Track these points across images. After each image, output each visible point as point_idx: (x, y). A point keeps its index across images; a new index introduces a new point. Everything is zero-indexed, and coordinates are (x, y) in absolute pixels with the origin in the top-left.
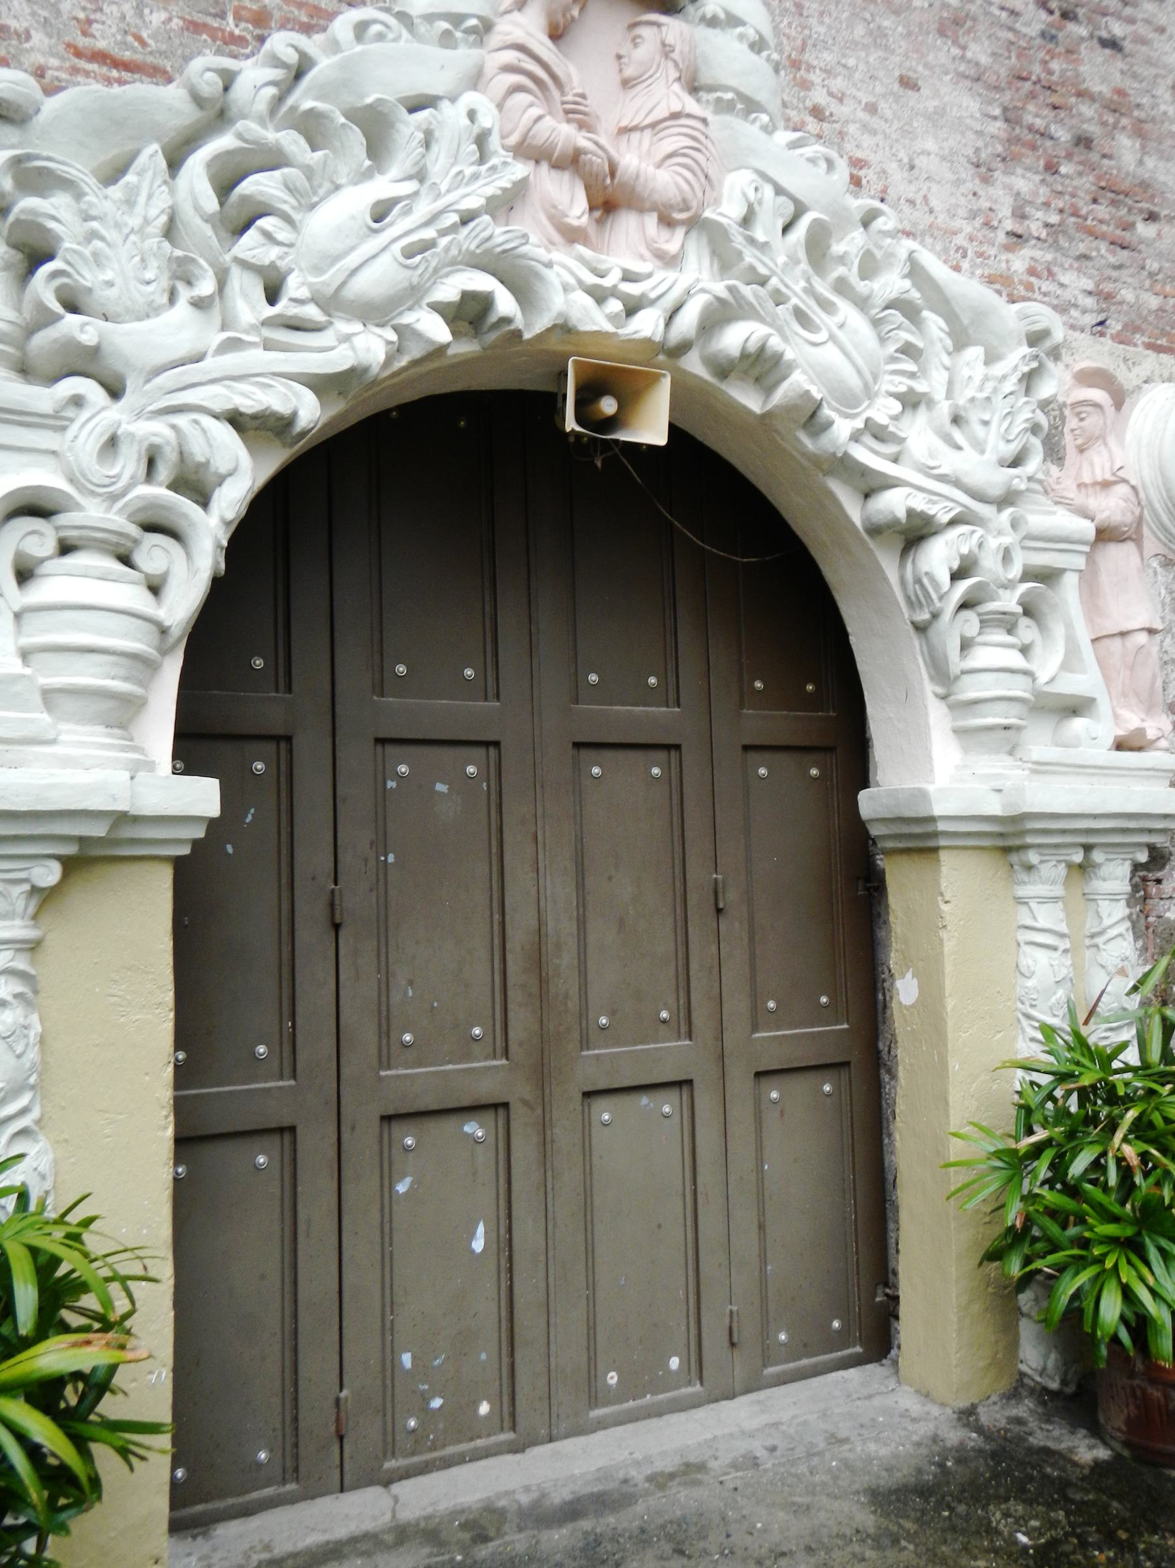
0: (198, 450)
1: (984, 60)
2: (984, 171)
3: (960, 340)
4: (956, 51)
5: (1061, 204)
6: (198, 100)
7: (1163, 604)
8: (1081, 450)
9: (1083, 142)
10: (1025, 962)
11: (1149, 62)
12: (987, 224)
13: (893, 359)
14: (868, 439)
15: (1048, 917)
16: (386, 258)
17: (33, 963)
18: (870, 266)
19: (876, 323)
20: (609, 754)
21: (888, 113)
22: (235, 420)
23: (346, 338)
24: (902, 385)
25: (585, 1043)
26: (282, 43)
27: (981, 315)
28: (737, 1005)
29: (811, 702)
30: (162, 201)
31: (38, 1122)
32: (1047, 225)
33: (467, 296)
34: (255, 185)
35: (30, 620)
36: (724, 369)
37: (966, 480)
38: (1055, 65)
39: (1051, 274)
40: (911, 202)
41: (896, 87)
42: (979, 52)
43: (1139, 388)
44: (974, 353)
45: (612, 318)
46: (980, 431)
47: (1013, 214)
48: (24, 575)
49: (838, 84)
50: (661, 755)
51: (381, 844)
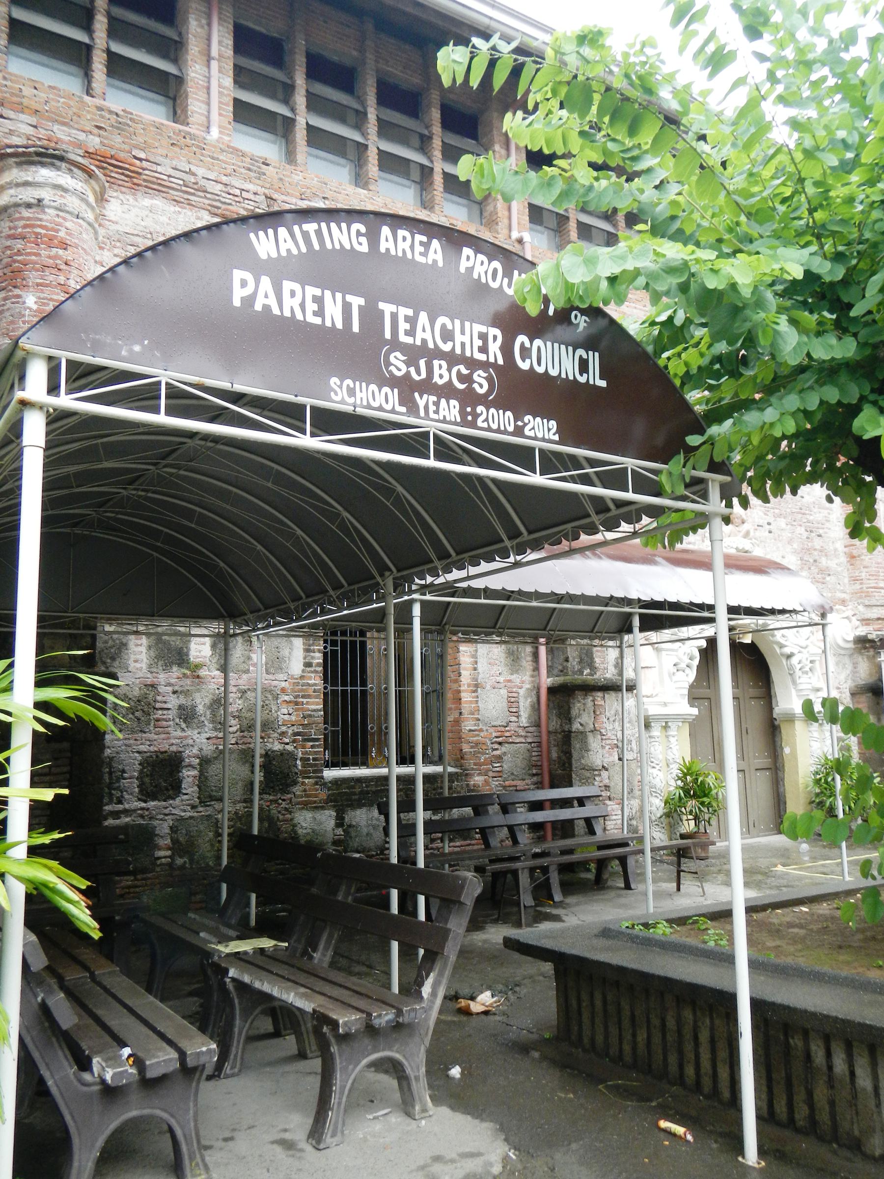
9: (815, 561)
15: (816, 734)
28: (751, 754)
29: (760, 687)
42: (795, 546)
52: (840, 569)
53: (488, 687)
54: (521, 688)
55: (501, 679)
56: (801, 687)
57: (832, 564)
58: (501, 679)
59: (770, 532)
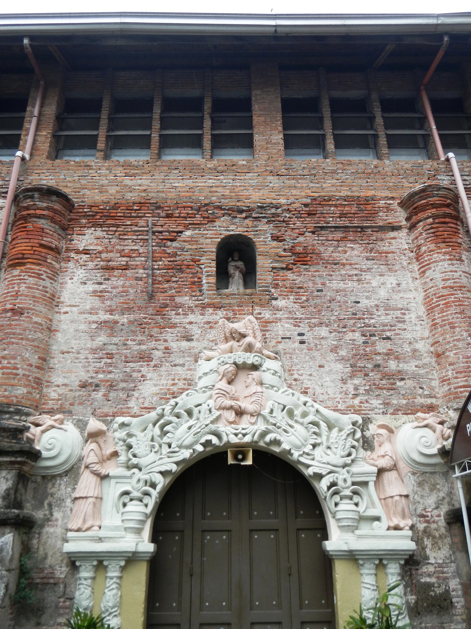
0: (153, 480)
1: (344, 354)
2: (344, 381)
3: (330, 427)
4: (336, 355)
5: (369, 384)
6: (158, 415)
7: (413, 486)
8: (380, 446)
10: (363, 593)
11: (400, 339)
12: (346, 394)
13: (311, 436)
14: (305, 456)
16: (190, 437)
17: (120, 581)
18: (305, 415)
19: (306, 428)
20: (259, 532)
21: (315, 375)
22: (161, 473)
23: (182, 453)
24: (313, 442)
25: (251, 609)
26: (172, 402)
27: (337, 420)
30: (151, 434)
31: (119, 614)
32: (365, 390)
33: (207, 441)
34: (166, 428)
35: (124, 515)
36: (268, 444)
37: (331, 463)
38: (368, 349)
39: (367, 402)
40: (323, 394)
41: (318, 368)
42: (343, 353)
43: (401, 426)
44: (336, 430)
46: (334, 450)
47: (354, 389)
48: (125, 505)
49: (300, 372)
50: (274, 532)
51: (202, 556)
52: (422, 371)
56: (339, 516)
59: (302, 342)
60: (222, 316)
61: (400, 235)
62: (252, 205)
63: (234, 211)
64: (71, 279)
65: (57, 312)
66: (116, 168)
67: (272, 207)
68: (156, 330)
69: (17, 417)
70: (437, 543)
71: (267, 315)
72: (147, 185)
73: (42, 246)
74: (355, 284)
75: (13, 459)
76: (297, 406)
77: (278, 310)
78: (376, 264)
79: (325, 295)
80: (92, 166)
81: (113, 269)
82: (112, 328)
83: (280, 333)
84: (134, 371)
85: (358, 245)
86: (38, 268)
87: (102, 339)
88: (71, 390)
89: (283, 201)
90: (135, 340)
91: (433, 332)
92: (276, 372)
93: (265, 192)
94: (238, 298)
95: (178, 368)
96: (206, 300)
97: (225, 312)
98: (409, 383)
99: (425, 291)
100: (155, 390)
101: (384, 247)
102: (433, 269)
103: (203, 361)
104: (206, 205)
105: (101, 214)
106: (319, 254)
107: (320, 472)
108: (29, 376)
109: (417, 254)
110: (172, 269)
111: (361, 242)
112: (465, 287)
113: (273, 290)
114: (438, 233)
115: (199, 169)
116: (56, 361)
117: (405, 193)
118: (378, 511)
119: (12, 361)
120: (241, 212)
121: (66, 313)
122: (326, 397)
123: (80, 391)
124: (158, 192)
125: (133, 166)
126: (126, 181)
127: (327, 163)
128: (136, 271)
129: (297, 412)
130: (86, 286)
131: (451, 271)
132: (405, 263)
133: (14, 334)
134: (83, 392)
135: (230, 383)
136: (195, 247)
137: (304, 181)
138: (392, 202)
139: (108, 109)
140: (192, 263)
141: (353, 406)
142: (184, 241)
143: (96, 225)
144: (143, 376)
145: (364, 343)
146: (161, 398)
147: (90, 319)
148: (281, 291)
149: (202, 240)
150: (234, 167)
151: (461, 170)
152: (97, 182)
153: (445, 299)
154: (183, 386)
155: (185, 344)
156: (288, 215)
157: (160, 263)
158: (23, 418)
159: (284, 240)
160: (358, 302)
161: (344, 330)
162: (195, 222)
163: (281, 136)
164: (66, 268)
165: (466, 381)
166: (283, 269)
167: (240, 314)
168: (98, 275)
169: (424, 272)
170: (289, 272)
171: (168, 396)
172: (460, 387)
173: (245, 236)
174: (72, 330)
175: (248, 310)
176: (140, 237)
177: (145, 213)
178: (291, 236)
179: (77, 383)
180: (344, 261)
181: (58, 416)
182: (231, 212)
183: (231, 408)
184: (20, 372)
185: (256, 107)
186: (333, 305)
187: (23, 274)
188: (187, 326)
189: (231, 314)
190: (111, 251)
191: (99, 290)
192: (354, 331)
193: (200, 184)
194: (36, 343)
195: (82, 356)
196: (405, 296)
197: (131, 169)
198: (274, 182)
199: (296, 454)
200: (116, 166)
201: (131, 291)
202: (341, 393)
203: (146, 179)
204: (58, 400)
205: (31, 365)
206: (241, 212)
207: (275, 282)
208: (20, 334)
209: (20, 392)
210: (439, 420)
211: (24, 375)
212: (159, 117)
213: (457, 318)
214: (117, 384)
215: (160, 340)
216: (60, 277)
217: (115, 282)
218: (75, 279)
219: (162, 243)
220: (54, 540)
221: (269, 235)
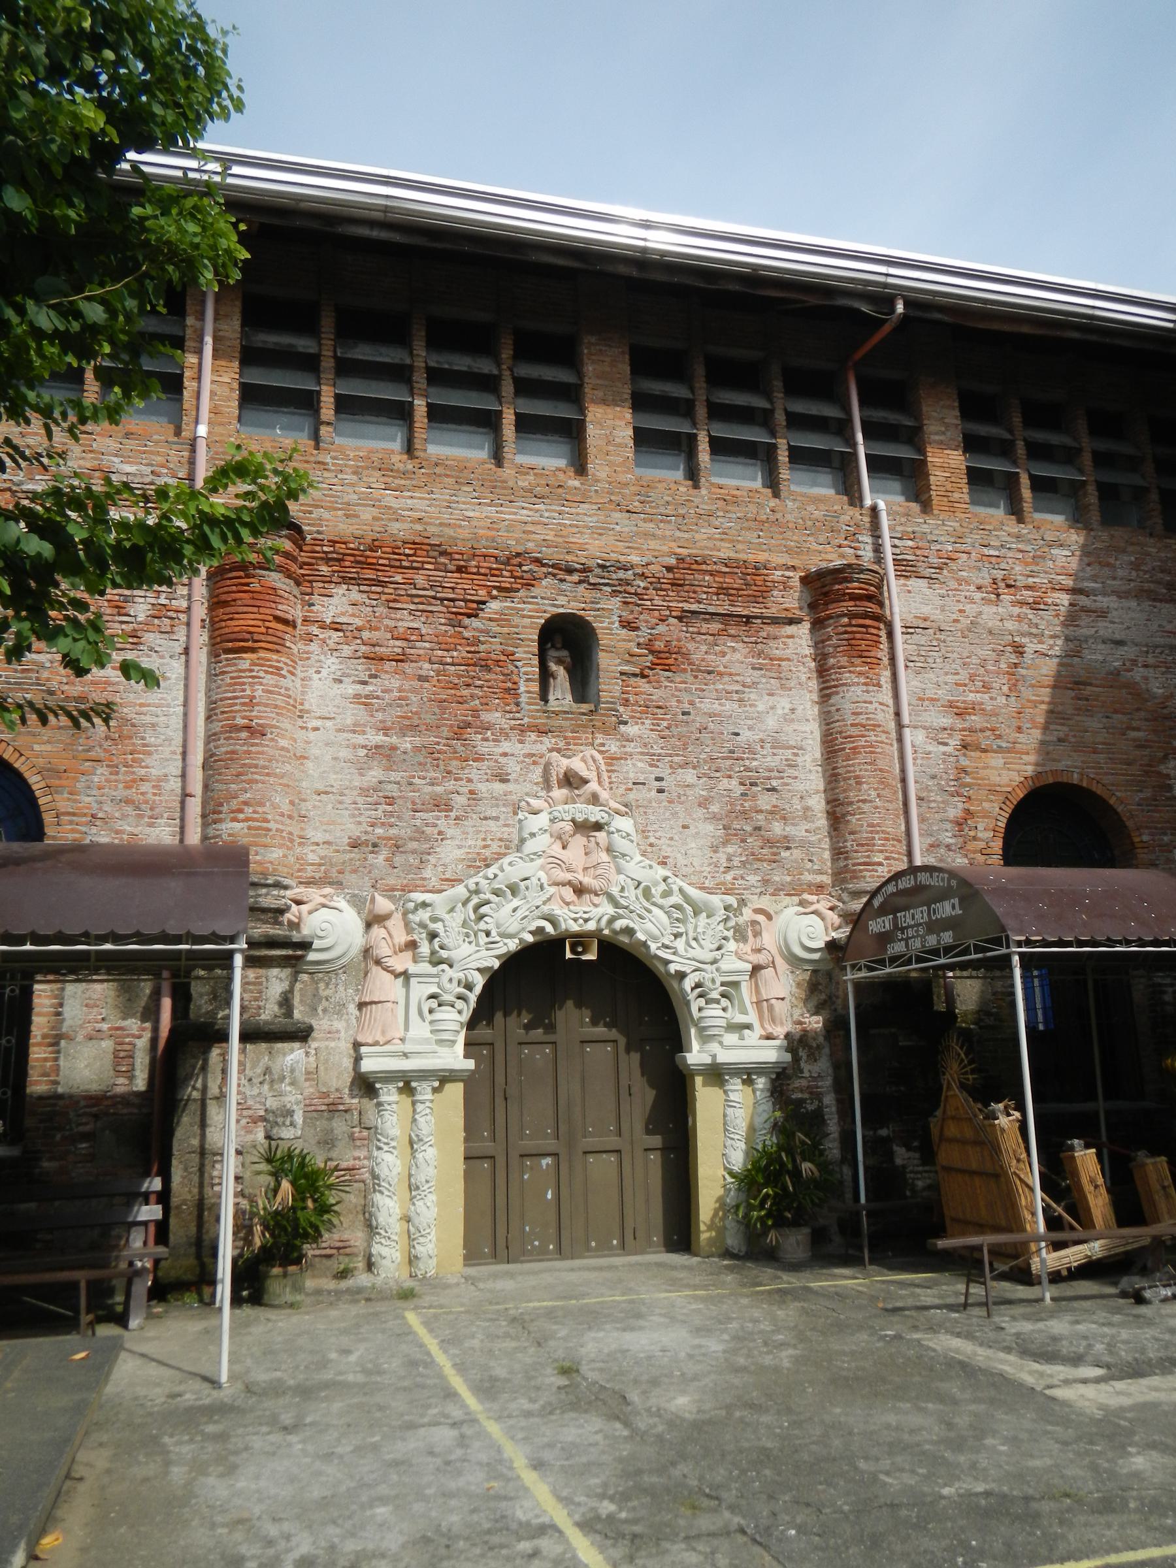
0: (470, 980)
22: (478, 969)
24: (675, 931)
26: (490, 872)
27: (706, 904)
34: (483, 910)
38: (746, 804)
42: (715, 808)
44: (704, 914)
45: (580, 926)
49: (657, 835)
53: (80, 1038)
54: (139, 1037)
55: (105, 1026)
57: (798, 831)
58: (105, 1026)
59: (661, 791)
60: (549, 746)
61: (801, 632)
62: (591, 563)
63: (561, 569)
64: (318, 672)
65: (302, 728)
66: (370, 472)
67: (619, 569)
68: (454, 763)
69: (275, 893)
70: (813, 1054)
71: (613, 747)
72: (422, 511)
73: (278, 619)
74: (735, 706)
75: (290, 952)
76: (656, 884)
77: (628, 740)
78: (764, 676)
79: (693, 721)
80: (326, 464)
81: (382, 659)
82: (389, 757)
83: (631, 775)
84: (427, 825)
85: (741, 645)
86: (275, 657)
87: (375, 774)
88: (338, 851)
89: (635, 559)
90: (424, 778)
91: (833, 785)
92: (628, 835)
93: (608, 540)
94: (571, 719)
95: (490, 822)
96: (526, 720)
97: (553, 740)
98: (797, 853)
99: (828, 724)
100: (460, 853)
101: (775, 649)
102: (842, 695)
103: (527, 814)
104: (518, 555)
105: (352, 559)
106: (686, 655)
107: (683, 969)
108: (282, 831)
109: (821, 666)
110: (474, 665)
111: (746, 639)
112: (879, 726)
113: (621, 709)
114: (853, 642)
115: (505, 488)
116: (309, 805)
117: (815, 564)
118: (752, 1017)
119: (260, 809)
120: (570, 571)
121: (316, 729)
122: (690, 870)
123: (351, 852)
124: (441, 524)
125: (398, 471)
126: (388, 499)
127: (702, 497)
128: (419, 664)
129: (656, 891)
130: (341, 685)
131: (865, 702)
132: (803, 678)
133: (256, 766)
134: (355, 854)
135: (564, 848)
136: (506, 630)
137: (667, 526)
138: (791, 574)
139: (332, 337)
140: (503, 658)
141: (724, 884)
142: (490, 620)
143: (345, 580)
144: (440, 833)
145: (742, 794)
146: (469, 866)
147: (353, 741)
148: (633, 711)
149: (516, 620)
150: (560, 490)
151: (891, 529)
152: (338, 497)
153: (853, 742)
154: (498, 850)
155: (498, 787)
156: (642, 584)
157: (455, 654)
158: (282, 892)
159: (637, 629)
160: (737, 734)
161: (718, 775)
162: (503, 585)
163: (630, 432)
164: (307, 653)
165: (868, 857)
166: (635, 675)
167: (575, 744)
168: (360, 668)
169: (829, 696)
170: (644, 680)
171: (478, 864)
172: (860, 864)
173: (581, 617)
174: (328, 757)
175: (587, 738)
176: (421, 607)
177: (423, 563)
178: (647, 622)
179: (346, 841)
180: (721, 669)
181: (328, 890)
182: (556, 571)
183: (569, 883)
184: (272, 825)
185: (589, 369)
186: (705, 736)
187: (256, 668)
188: (501, 759)
189: (561, 745)
190: (377, 629)
191: (363, 693)
192: (730, 777)
193: (507, 517)
194: (285, 781)
195: (348, 799)
196: (800, 728)
197: (394, 477)
198: (623, 523)
199: (653, 947)
200: (367, 468)
201: (414, 698)
202: (710, 864)
203: (420, 498)
204: (320, 865)
205: (282, 815)
206: (570, 571)
207: (625, 696)
208: (264, 767)
209: (275, 855)
210: (830, 904)
211: (277, 830)
212: (423, 365)
213: (866, 770)
214: (405, 844)
215: (461, 779)
216: (299, 668)
217: (386, 682)
218: (324, 672)
219: (455, 620)
220: (337, 1058)
221: (616, 619)
